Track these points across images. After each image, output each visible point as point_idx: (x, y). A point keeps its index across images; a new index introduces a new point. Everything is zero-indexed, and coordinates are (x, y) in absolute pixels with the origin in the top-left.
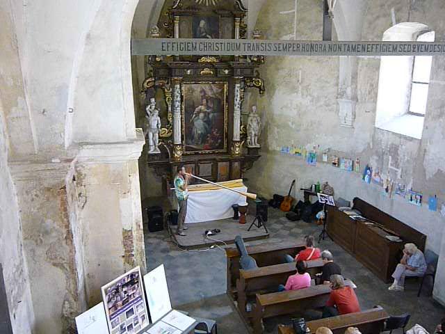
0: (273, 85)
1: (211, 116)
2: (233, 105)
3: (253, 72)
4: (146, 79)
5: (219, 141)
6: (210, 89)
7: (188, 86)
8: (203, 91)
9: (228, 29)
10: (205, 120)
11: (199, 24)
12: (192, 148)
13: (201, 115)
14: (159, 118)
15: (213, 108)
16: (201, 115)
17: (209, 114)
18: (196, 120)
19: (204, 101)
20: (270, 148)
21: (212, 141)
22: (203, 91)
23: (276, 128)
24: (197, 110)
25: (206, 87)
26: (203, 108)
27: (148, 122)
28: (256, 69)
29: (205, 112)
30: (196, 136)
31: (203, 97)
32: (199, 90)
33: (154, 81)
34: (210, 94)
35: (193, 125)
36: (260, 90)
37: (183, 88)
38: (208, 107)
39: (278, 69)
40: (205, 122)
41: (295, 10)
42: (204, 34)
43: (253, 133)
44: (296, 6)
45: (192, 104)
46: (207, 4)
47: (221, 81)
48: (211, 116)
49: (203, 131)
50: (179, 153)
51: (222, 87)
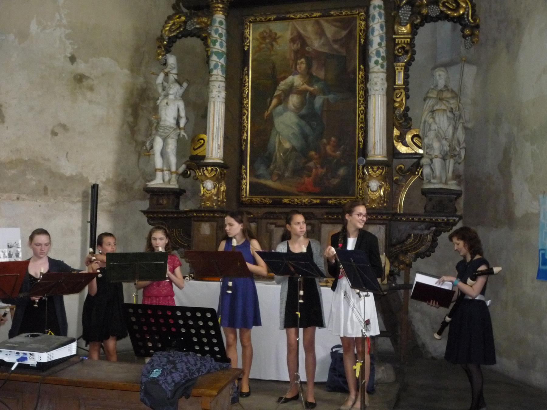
0: (518, 23)
1: (318, 101)
5: (342, 171)
7: (262, 28)
8: (299, 39)
10: (304, 111)
12: (265, 186)
13: (294, 100)
14: (181, 104)
16: (294, 100)
17: (313, 95)
18: (281, 114)
19: (302, 64)
20: (519, 212)
21: (321, 171)
22: (299, 39)
23: (528, 144)
24: (282, 85)
25: (308, 29)
26: (297, 80)
27: (156, 109)
29: (302, 93)
30: (279, 155)
32: (288, 35)
33: (185, 23)
34: (316, 44)
36: (465, 26)
38: (310, 78)
40: (302, 117)
43: (436, 145)
47: (346, 8)
48: (318, 101)
49: (297, 143)
50: (209, 184)
51: (347, 23)
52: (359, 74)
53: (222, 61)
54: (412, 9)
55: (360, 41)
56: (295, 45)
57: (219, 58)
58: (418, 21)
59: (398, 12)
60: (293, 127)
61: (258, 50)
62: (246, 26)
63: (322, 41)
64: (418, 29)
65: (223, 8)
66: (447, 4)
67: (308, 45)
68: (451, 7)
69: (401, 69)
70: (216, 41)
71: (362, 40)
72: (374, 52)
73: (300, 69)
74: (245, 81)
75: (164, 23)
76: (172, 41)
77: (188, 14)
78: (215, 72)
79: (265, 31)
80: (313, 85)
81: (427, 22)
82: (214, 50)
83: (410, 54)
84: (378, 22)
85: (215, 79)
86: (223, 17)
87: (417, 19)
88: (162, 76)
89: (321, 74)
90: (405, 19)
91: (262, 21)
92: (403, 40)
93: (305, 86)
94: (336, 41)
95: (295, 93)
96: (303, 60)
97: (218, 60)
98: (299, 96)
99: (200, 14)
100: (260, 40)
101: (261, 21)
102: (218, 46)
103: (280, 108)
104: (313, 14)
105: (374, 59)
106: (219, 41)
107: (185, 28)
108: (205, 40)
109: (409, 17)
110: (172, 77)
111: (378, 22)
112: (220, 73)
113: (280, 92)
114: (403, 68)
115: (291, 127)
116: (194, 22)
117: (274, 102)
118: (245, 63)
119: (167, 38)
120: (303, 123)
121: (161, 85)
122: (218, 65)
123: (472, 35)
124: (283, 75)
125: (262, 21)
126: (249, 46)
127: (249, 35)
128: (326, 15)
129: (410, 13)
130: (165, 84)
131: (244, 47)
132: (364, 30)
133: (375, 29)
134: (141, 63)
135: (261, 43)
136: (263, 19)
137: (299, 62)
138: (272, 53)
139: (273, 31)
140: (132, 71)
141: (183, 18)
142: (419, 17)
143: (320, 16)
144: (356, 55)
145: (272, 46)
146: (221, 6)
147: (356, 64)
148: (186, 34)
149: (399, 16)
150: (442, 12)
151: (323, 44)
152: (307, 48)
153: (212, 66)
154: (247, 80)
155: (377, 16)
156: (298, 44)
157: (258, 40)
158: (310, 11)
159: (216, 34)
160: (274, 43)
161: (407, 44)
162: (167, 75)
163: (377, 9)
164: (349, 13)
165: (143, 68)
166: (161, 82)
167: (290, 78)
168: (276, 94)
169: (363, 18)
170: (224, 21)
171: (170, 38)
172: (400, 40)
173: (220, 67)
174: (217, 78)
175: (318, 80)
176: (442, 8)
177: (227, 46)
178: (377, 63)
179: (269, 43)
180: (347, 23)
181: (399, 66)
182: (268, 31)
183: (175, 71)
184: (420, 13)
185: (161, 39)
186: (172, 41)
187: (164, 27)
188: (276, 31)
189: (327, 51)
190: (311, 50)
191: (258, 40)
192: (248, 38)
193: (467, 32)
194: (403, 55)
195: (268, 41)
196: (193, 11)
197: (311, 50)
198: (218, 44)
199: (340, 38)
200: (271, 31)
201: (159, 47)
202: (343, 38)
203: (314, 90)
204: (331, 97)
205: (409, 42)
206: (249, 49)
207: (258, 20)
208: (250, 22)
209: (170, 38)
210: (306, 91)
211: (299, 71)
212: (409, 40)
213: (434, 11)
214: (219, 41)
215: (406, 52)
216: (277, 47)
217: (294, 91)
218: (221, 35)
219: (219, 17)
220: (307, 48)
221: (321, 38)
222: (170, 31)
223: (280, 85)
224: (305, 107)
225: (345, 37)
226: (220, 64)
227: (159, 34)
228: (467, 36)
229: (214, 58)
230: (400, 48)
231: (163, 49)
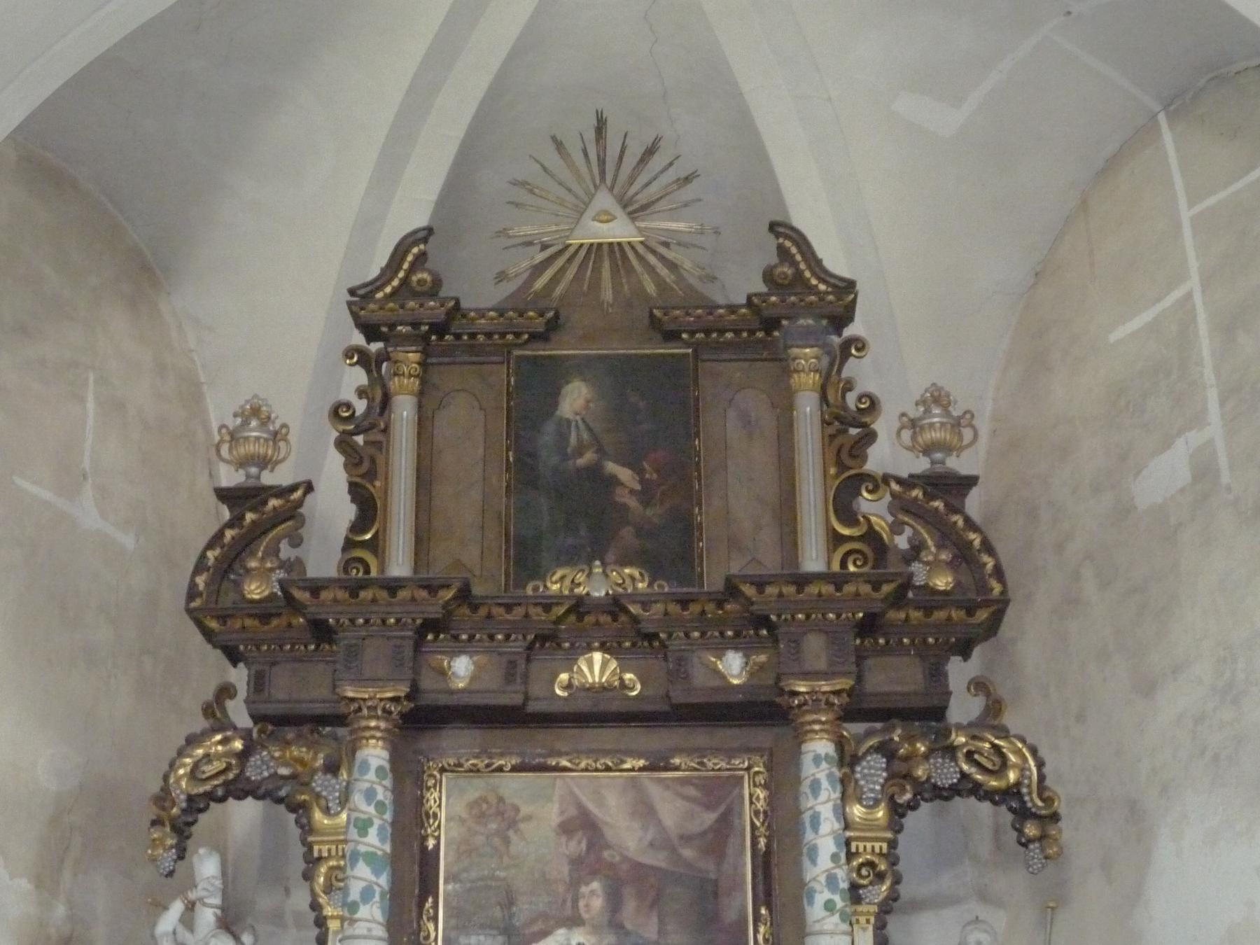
2: (802, 892)
3: (937, 674)
4: (192, 741)
6: (633, 803)
7: (475, 788)
8: (583, 824)
9: (747, 422)
11: (555, 404)
19: (594, 897)
22: (583, 824)
28: (959, 672)
31: (584, 867)
32: (552, 814)
33: (244, 756)
36: (1023, 814)
37: (446, 803)
39: (1147, 687)
41: (1194, 283)
42: (588, 457)
44: (1194, 264)
46: (607, 295)
47: (716, 751)
52: (756, 931)
53: (384, 880)
54: (888, 763)
55: (754, 843)
56: (573, 844)
57: (377, 873)
58: (908, 796)
59: (853, 772)
61: (465, 850)
62: (431, 782)
63: (649, 836)
64: (903, 816)
65: (386, 730)
66: (976, 756)
68: (989, 766)
69: (868, 921)
70: (369, 823)
71: (762, 842)
72: (823, 879)
74: (427, 937)
75: (175, 755)
76: (197, 805)
77: (255, 735)
78: (363, 912)
79: (484, 800)
81: (926, 800)
82: (362, 849)
83: (888, 883)
84: (828, 800)
85: (365, 932)
86: (385, 754)
87: (903, 791)
88: (177, 908)
90: (872, 790)
91: (478, 771)
92: (869, 845)
96: (595, 885)
97: (374, 879)
99: (290, 736)
101: (475, 770)
102: (373, 837)
104: (623, 762)
105: (822, 896)
106: (377, 822)
107: (242, 772)
108: (299, 809)
109: (883, 786)
110: (207, 917)
111: (828, 800)
112: (378, 915)
114: (872, 920)
116: (273, 757)
118: (428, 886)
119: (183, 797)
121: (171, 937)
122: (374, 891)
123: (1042, 838)
125: (478, 771)
126: (438, 838)
127: (440, 806)
128: (657, 764)
129: (885, 774)
130: (184, 935)
131: (424, 838)
132: (765, 812)
133: (822, 817)
134: (62, 861)
136: (481, 765)
137: (584, 889)
139: (507, 801)
140: (39, 882)
141: (238, 745)
142: (908, 787)
143: (640, 769)
144: (744, 875)
145: (507, 841)
146: (383, 725)
147: (745, 907)
148: (238, 789)
149: (857, 781)
150: (964, 776)
151: (651, 844)
152: (606, 854)
153: (354, 894)
154: (433, 935)
155: (825, 784)
156: (580, 842)
157: (462, 821)
158: (618, 751)
159: (369, 805)
160: (511, 833)
161: (881, 854)
162: (191, 907)
163: (824, 765)
164: (723, 765)
165: (67, 876)
166: (170, 929)
169: (760, 779)
170: (387, 766)
171: (191, 799)
172: (861, 845)
173: (377, 898)
174: (369, 930)
176: (965, 767)
177: (393, 841)
178: (829, 906)
180: (717, 792)
181: (862, 913)
182: (493, 800)
183: (217, 901)
184: (907, 776)
185: (163, 798)
186: (197, 805)
187: (172, 766)
188: (516, 801)
189: (663, 865)
190: (618, 858)
191: (462, 821)
192: (435, 815)
193: (1031, 830)
194: (871, 883)
195: (494, 826)
196: (270, 727)
198: (373, 832)
200: (501, 800)
201: (154, 823)
202: (704, 833)
205: (885, 851)
206: (437, 846)
207: (467, 765)
208: (443, 770)
209: (191, 799)
211: (585, 916)
212: (885, 846)
213: (946, 774)
214: (377, 822)
215: (880, 877)
216: (517, 845)
218: (380, 806)
219: (375, 754)
220: (606, 854)
221: (645, 828)
222: (193, 775)
225: (710, 829)
226: (377, 889)
227: (155, 786)
228: (1030, 841)
229: (363, 870)
230: (862, 865)
231: (168, 829)
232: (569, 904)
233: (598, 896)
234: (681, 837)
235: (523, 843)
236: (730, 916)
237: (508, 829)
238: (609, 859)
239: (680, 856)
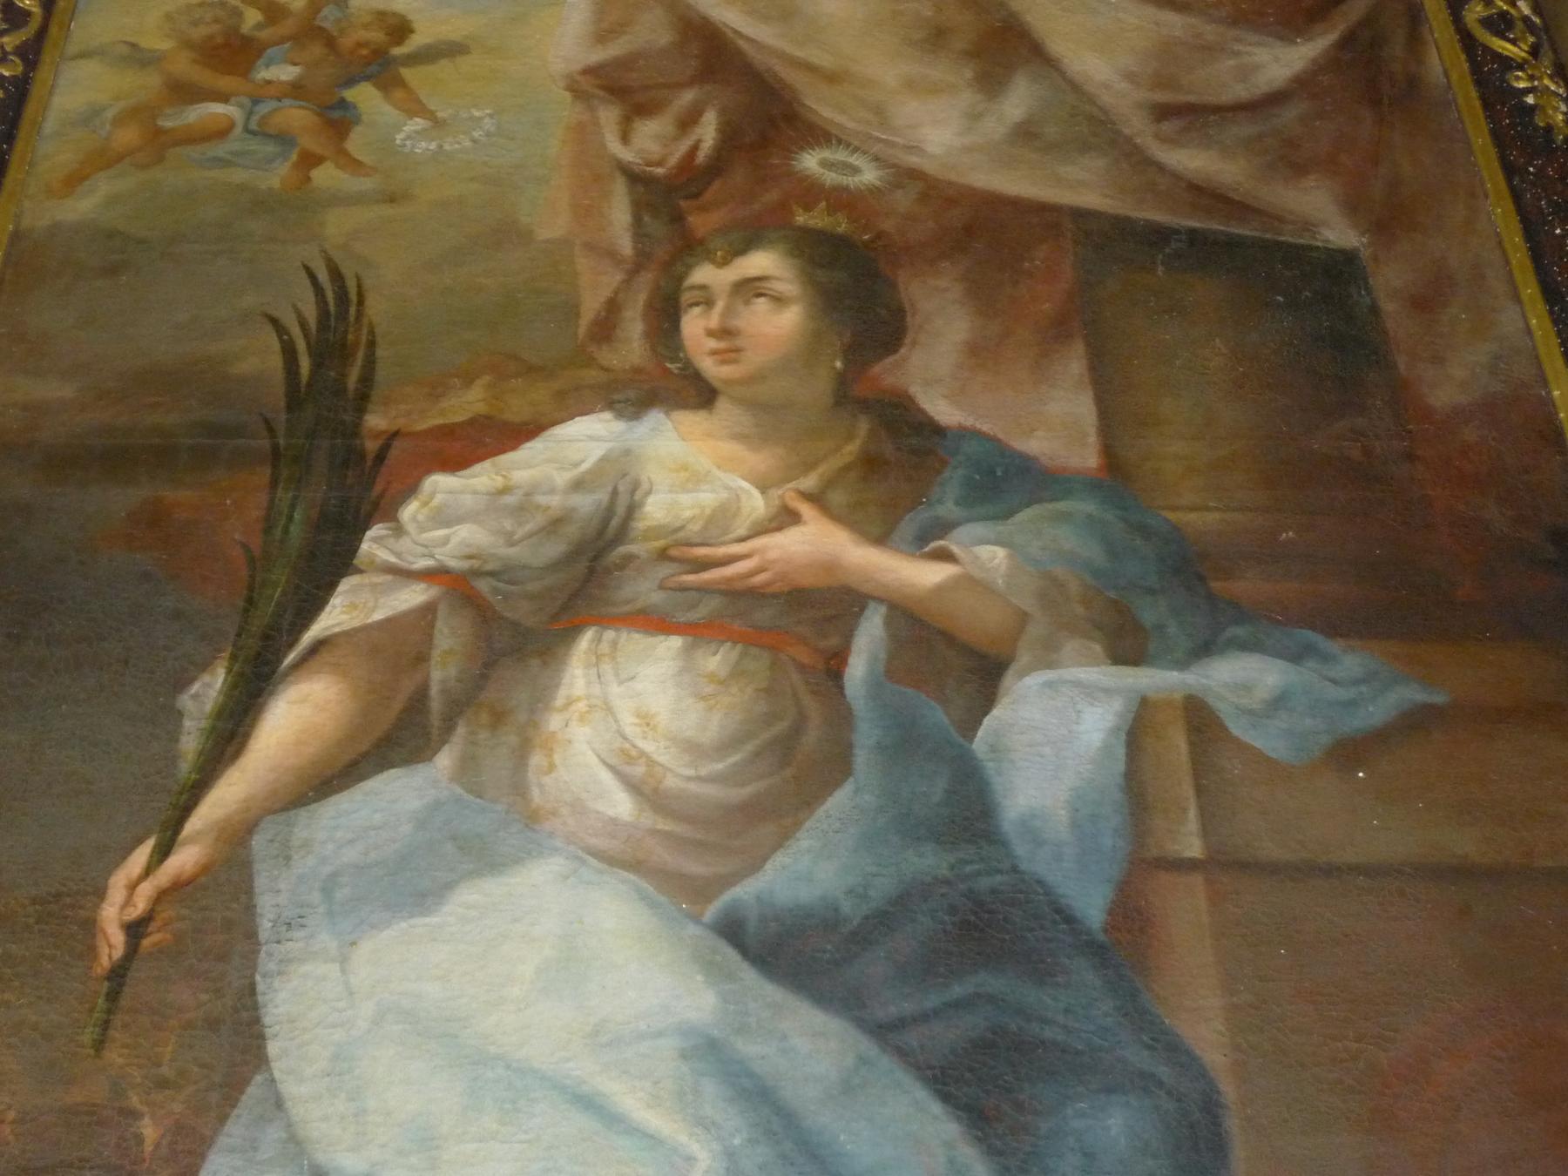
1: (1056, 735)
10: (812, 866)
15: (1117, 474)
16: (634, 709)
18: (410, 883)
19: (757, 305)
24: (448, 520)
26: (690, 474)
35: (236, 1047)
38: (898, 463)
45: (259, 359)
48: (1056, 735)
60: (631, 1101)
67: (818, 135)
73: (729, 355)
80: (944, 528)
89: (1056, 419)
93: (818, 543)
94: (1187, 116)
95: (655, 622)
96: (760, 262)
98: (716, 660)
100: (184, 66)
103: (397, 797)
113: (413, 596)
115: (589, 1103)
117: (300, 715)
120: (808, 1045)
124: (468, 403)
135: (184, 92)
138: (326, 176)
145: (338, 120)
151: (1025, 133)
157: (137, 58)
160: (364, 96)
167: (586, 438)
168: (335, 617)
175: (1005, 482)
179: (296, 90)
189: (1091, 199)
195: (286, 73)
197: (869, 175)
199: (1240, 92)
202: (1276, 99)
203: (968, 582)
204: (1241, 680)
210: (825, 607)
217: (644, 589)
221: (991, 82)
223: (409, 512)
224: (840, 800)
225: (1303, 84)
232: (634, 328)
233: (779, 301)
234: (1163, 112)
235: (419, 123)
236: (1452, 379)
237: (351, 82)
238: (831, 178)
239: (1161, 168)
